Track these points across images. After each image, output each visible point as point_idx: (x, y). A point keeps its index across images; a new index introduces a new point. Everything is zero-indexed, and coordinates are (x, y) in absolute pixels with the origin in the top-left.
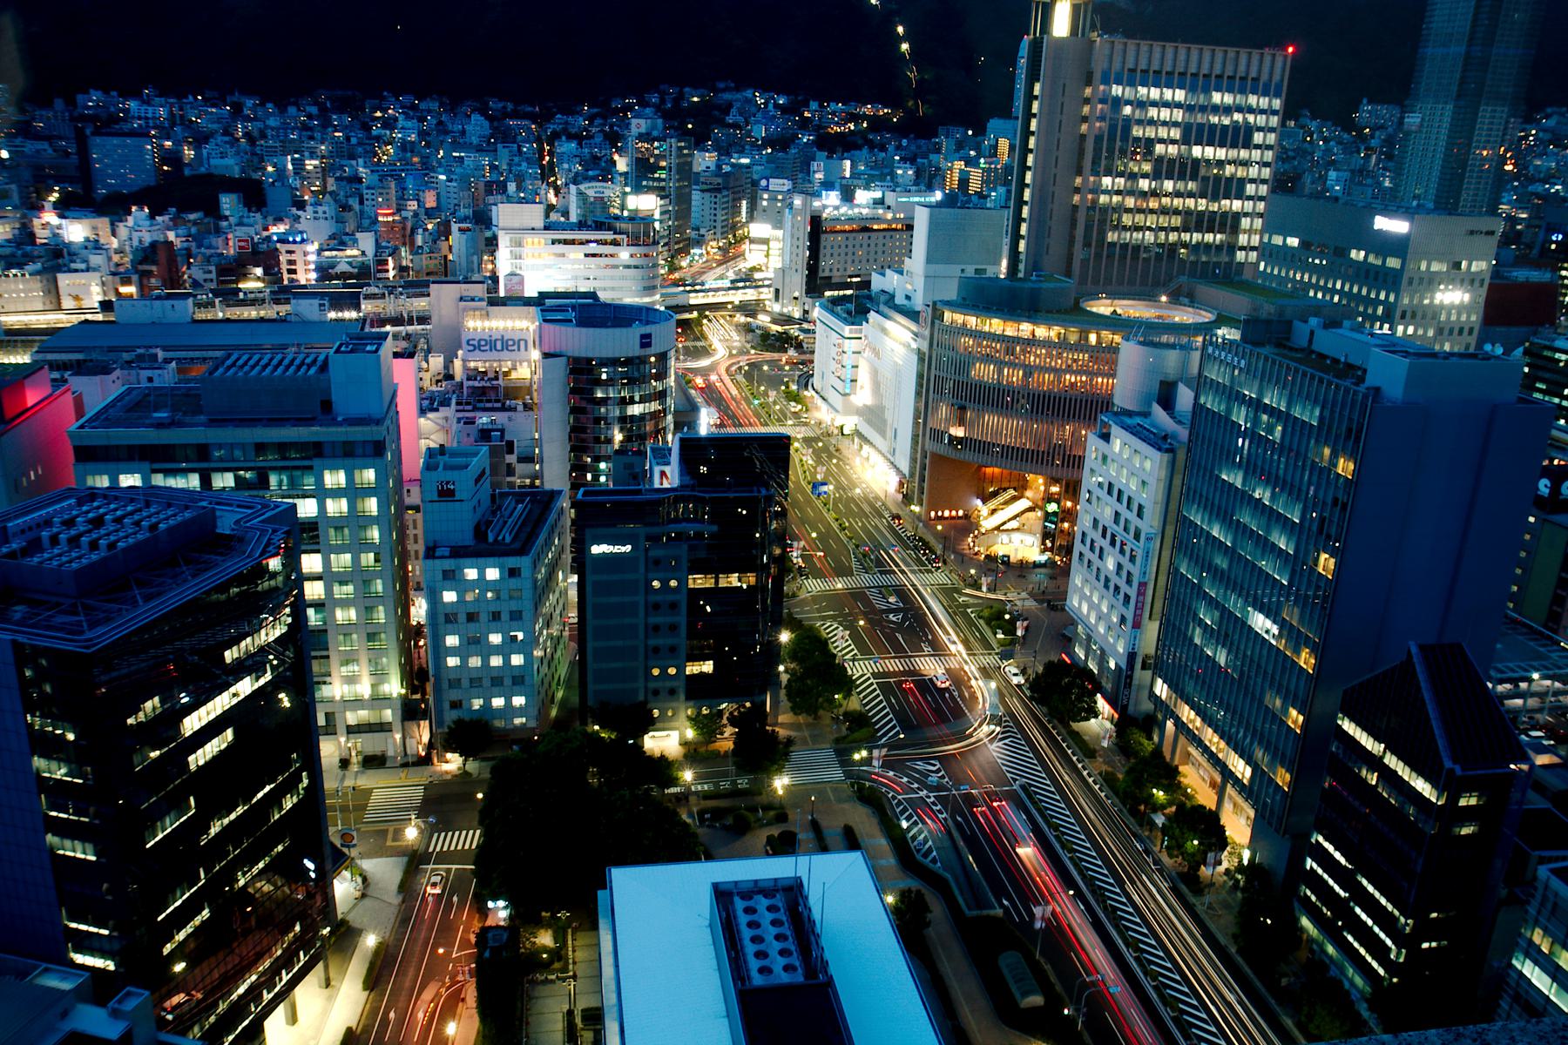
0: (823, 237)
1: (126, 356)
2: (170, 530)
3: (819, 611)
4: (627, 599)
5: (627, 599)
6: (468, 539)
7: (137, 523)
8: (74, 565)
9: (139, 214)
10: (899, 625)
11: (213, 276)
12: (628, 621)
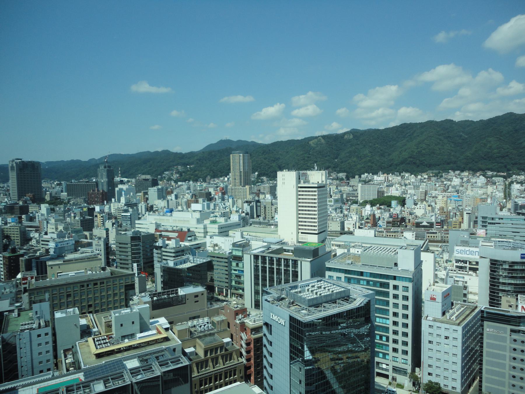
1: (353, 245)
2: (336, 293)
6: (439, 315)
7: (329, 290)
8: (310, 298)
9: (368, 207)
11: (385, 224)
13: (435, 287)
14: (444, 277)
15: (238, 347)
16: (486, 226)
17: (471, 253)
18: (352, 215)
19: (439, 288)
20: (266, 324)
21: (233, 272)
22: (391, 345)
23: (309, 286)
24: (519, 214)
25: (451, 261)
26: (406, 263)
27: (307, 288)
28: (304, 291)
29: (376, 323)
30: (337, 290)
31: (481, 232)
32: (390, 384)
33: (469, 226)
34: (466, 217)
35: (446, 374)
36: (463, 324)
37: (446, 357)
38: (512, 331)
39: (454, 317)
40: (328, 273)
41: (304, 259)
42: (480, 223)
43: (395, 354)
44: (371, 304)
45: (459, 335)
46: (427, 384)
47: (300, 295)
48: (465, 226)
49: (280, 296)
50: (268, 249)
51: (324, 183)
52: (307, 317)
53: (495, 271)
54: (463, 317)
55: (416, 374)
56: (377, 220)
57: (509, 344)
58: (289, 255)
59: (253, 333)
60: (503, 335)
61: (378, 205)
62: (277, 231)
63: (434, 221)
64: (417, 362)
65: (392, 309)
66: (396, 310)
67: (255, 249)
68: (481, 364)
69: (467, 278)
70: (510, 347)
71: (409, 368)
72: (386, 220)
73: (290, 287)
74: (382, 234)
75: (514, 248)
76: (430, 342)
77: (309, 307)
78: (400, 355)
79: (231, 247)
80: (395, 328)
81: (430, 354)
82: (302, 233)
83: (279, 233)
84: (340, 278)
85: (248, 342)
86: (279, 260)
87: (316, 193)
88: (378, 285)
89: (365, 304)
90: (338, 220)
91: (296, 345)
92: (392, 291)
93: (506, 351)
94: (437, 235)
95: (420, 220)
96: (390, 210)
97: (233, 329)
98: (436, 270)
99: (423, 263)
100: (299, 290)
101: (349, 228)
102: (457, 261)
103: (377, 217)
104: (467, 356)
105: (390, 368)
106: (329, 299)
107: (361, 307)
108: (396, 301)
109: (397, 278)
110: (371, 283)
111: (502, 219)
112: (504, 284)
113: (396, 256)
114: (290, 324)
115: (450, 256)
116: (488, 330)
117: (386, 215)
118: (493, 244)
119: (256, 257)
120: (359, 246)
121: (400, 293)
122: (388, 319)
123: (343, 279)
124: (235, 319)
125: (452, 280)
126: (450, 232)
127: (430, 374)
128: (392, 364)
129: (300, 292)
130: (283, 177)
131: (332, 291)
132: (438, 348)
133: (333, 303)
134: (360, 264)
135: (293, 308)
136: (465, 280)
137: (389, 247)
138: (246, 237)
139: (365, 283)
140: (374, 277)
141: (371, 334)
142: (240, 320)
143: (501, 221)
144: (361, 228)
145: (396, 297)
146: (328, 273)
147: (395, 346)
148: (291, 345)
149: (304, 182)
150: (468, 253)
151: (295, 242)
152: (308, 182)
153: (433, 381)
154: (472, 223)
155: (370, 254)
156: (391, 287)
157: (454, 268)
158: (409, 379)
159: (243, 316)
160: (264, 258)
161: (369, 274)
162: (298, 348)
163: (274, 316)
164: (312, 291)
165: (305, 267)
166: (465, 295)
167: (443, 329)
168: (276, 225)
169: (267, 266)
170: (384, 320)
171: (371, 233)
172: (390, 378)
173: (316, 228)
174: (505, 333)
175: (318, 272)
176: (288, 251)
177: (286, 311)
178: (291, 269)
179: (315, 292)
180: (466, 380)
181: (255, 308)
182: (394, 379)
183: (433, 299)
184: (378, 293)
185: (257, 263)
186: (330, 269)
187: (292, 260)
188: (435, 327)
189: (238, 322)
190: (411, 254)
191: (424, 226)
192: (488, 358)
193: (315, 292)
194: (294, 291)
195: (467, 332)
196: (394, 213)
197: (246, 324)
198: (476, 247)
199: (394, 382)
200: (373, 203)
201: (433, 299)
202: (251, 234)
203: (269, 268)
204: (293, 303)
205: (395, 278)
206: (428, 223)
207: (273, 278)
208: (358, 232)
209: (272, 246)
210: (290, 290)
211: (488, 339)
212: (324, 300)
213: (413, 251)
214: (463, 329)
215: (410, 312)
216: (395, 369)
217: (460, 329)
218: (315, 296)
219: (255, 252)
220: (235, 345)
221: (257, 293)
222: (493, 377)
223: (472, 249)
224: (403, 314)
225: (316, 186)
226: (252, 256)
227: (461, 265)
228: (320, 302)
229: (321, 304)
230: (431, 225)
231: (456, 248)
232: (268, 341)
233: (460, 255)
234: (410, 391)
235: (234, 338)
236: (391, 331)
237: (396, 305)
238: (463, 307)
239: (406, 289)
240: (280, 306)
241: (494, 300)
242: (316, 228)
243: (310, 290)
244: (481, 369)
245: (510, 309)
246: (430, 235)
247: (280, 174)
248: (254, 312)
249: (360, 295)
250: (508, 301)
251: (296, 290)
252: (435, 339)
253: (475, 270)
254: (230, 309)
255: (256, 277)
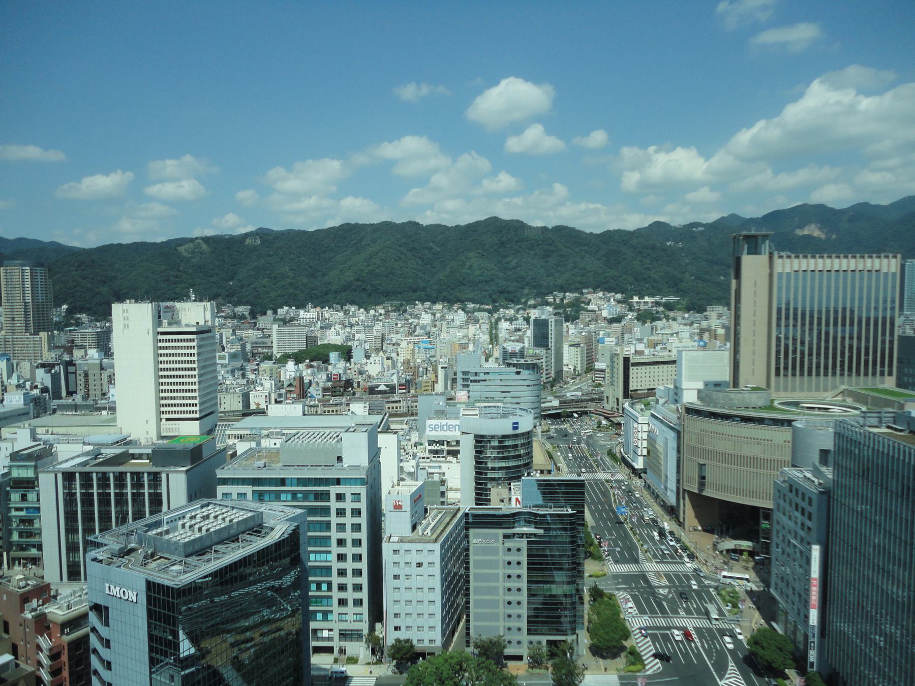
0: (631, 368)
1: (266, 432)
2: (238, 523)
3: (616, 584)
4: (492, 571)
5: (492, 571)
6: (407, 532)
8: (187, 540)
9: (291, 365)
10: (665, 596)
11: (320, 392)
12: (493, 584)
13: (400, 488)
14: (412, 470)
15: (30, 669)
16: (467, 386)
17: (450, 428)
18: (263, 381)
19: (405, 488)
20: (96, 608)
21: (14, 513)
22: (336, 595)
23: (184, 518)
24: (509, 365)
25: (422, 444)
26: (355, 454)
27: (180, 523)
28: (176, 529)
29: (310, 564)
30: (239, 516)
31: (461, 395)
32: (336, 661)
33: (446, 388)
34: (441, 373)
35: (420, 622)
36: (442, 539)
37: (420, 596)
38: (506, 536)
39: (428, 530)
40: (221, 490)
41: (172, 468)
42: (460, 382)
43: (343, 609)
44: (301, 531)
45: (436, 558)
46: (393, 646)
47: (166, 537)
48: (440, 387)
49: (126, 546)
50: (96, 458)
51: (209, 324)
52: (182, 577)
53: (481, 452)
54: (441, 528)
55: (377, 633)
56: (306, 387)
57: (503, 557)
58: (143, 465)
59: (67, 630)
60: (495, 545)
61: (307, 361)
62: (115, 420)
63: (395, 382)
64: (377, 614)
65: (335, 535)
66: (341, 536)
67: (66, 461)
68: (467, 595)
69: (445, 467)
70: (504, 561)
71: (364, 627)
72: (321, 385)
73: (146, 526)
74: (315, 409)
75: (504, 416)
76: (396, 577)
77: (186, 557)
78: (350, 609)
79: (7, 462)
80: (342, 565)
81: (397, 596)
82: (168, 420)
83: (119, 423)
84: (245, 494)
85: (54, 652)
86: (120, 478)
87: (194, 344)
88: (312, 497)
89: (290, 534)
90: (237, 390)
91: (162, 635)
92: (334, 505)
93: (498, 568)
94: (401, 404)
95: (375, 383)
96: (327, 369)
97: (16, 634)
98: (401, 460)
99: (382, 452)
100: (165, 528)
101: (258, 404)
102: (431, 443)
103: (306, 381)
104: (448, 587)
105: (336, 634)
106: (225, 535)
107: (284, 540)
108: (341, 520)
109: (342, 481)
110: (299, 495)
111: (488, 373)
112: (493, 469)
113: (339, 445)
114: (149, 598)
115: (420, 436)
116: (475, 541)
117: (322, 377)
118: (477, 412)
119: (69, 476)
120: (277, 433)
121: (348, 505)
122: (330, 552)
123: (250, 496)
124: (22, 610)
125: (424, 472)
126: (419, 398)
127: (396, 628)
128: (337, 626)
129: (167, 532)
130: (125, 315)
131: (231, 521)
132: (408, 584)
133: (233, 541)
134: (280, 464)
135: (153, 565)
136: (442, 471)
137: (328, 431)
138: (44, 437)
139: (289, 497)
140: (304, 486)
141: (301, 584)
142: (35, 610)
143: (486, 377)
144: (280, 402)
145: (341, 513)
146: (221, 490)
147: (342, 595)
148: (151, 637)
149: (170, 324)
150: (445, 428)
151: (155, 438)
152: (178, 323)
153: (402, 638)
154: (449, 383)
155: (295, 445)
156: (333, 497)
157: (427, 454)
158: (365, 645)
159: (41, 602)
160: (86, 478)
161: (295, 482)
162: (166, 640)
163: (112, 587)
164: (191, 527)
165: (176, 483)
166: (443, 494)
167: (414, 552)
168: (112, 409)
169: (95, 491)
170: (323, 555)
171: (296, 409)
172: (336, 650)
173: (197, 408)
174: (497, 541)
175: (202, 489)
176: (140, 456)
177: (138, 574)
178: (146, 491)
179: (197, 526)
180: (448, 625)
181: (69, 579)
182: (342, 651)
183: (398, 507)
184: (312, 511)
185: (70, 488)
186: (225, 481)
187: (149, 474)
188: (402, 552)
189: (29, 615)
190: (362, 439)
191: (382, 392)
192: (475, 584)
193: (197, 526)
194: (154, 532)
195: (448, 550)
196: (334, 372)
197: (49, 617)
198: (456, 418)
199: (343, 656)
200: (298, 358)
201: (398, 507)
202: (55, 430)
203: (99, 494)
204: (152, 555)
205: (338, 482)
206: (387, 386)
207: (109, 513)
208: (275, 410)
209: (103, 451)
210: (146, 532)
211: (474, 554)
212: (216, 539)
213: (366, 434)
214: (442, 547)
215: (363, 535)
216: (344, 635)
217: (437, 547)
218: (198, 535)
219: (66, 466)
220: (23, 665)
221: (72, 548)
222: (484, 611)
223: (450, 422)
224: (353, 540)
225: (194, 329)
226: (60, 476)
227: (436, 448)
228: (208, 543)
229: (210, 547)
230: (392, 389)
231: (429, 422)
232: (101, 639)
233: (434, 433)
234: (369, 664)
235: (21, 651)
236: (335, 572)
237: (341, 527)
238: (440, 513)
239: (356, 497)
240: (126, 566)
241: (481, 496)
242: (197, 408)
243: (187, 525)
244: (468, 602)
245: (502, 506)
246: (391, 405)
247: (116, 308)
248: (66, 590)
249: (279, 520)
250: (499, 494)
251: (159, 530)
252: (402, 571)
253: (455, 453)
254: (10, 594)
255: (70, 517)
